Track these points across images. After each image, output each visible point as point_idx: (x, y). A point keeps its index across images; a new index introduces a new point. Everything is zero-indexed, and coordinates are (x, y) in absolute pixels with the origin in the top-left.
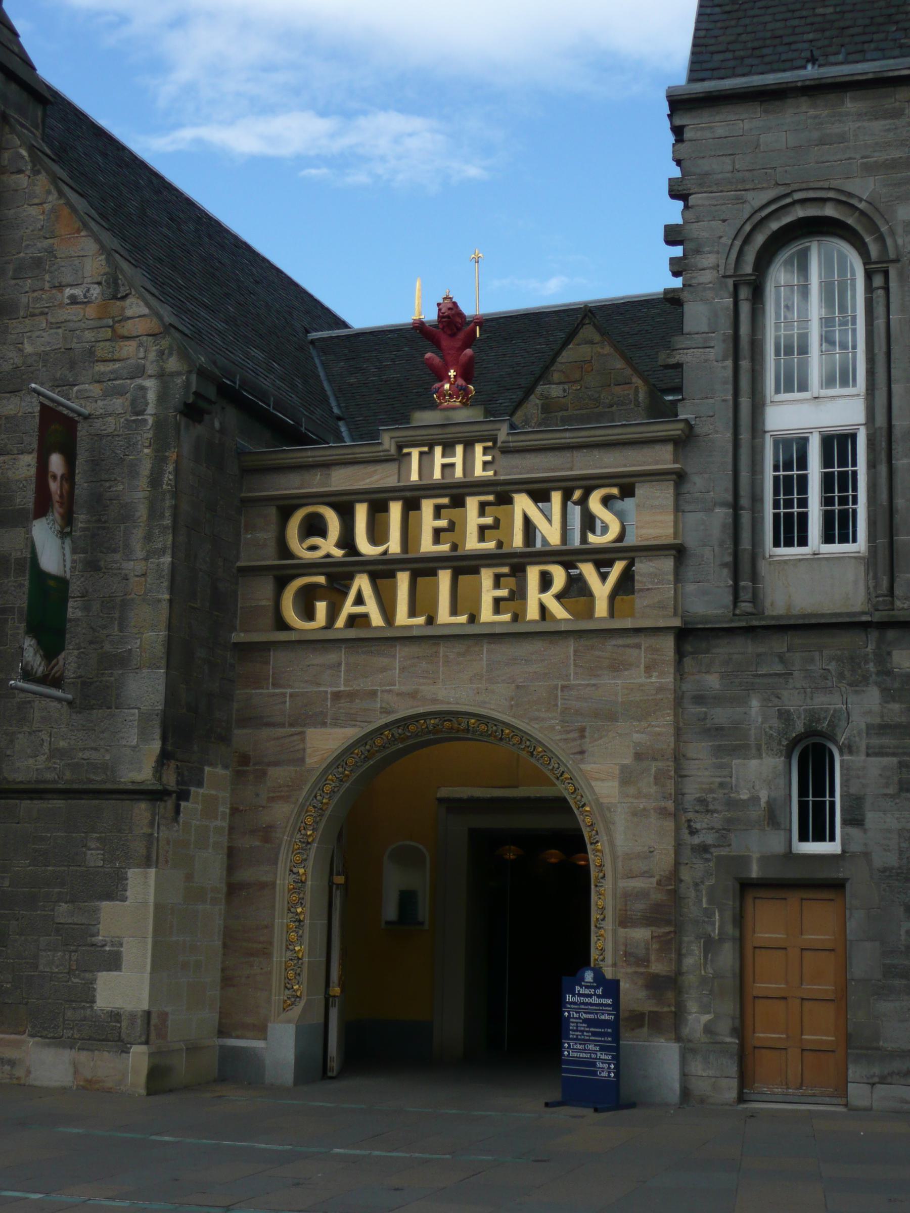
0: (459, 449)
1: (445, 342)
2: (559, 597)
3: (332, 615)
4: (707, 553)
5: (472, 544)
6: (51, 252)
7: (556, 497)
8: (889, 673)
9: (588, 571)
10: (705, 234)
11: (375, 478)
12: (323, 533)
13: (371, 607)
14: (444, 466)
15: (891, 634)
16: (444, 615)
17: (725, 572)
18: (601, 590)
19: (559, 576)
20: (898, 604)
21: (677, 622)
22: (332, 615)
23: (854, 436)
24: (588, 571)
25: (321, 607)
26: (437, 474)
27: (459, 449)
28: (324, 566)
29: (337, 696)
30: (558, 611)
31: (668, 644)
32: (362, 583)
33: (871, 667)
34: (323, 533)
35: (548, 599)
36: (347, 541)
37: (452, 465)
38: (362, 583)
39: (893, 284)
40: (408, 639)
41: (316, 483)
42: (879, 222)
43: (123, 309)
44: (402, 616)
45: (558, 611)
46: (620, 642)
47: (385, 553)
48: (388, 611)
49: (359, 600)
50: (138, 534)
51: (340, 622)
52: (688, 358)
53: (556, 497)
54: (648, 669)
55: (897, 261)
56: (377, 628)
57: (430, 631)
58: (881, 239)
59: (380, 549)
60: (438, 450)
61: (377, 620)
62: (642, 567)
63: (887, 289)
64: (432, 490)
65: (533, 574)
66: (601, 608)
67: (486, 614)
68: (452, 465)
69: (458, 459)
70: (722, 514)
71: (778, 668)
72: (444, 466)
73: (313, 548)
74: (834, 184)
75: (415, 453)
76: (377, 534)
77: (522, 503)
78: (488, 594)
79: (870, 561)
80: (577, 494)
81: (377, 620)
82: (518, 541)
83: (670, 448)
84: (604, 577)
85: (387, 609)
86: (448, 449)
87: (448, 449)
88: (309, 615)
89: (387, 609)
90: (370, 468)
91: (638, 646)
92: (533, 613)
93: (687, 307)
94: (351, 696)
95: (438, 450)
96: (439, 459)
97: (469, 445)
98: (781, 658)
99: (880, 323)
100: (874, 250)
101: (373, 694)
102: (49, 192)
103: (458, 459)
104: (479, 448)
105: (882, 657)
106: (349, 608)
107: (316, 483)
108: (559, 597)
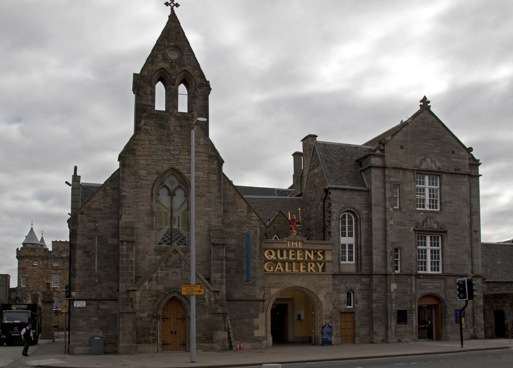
0: (296, 242)
1: (293, 223)
2: (313, 268)
3: (274, 269)
4: (335, 262)
5: (298, 258)
6: (235, 201)
7: (312, 252)
8: (361, 282)
9: (318, 264)
10: (334, 211)
11: (282, 246)
12: (272, 255)
13: (281, 268)
14: (294, 245)
15: (361, 276)
16: (294, 270)
17: (338, 265)
18: (320, 267)
19: (313, 265)
20: (362, 272)
21: (333, 273)
22: (274, 269)
23: (352, 245)
24: (318, 264)
25: (272, 268)
26: (293, 246)
27: (296, 242)
28: (272, 260)
29: (276, 283)
30: (314, 271)
31: (331, 276)
32: (279, 264)
33: (359, 281)
34: (272, 255)
35: (312, 268)
36: (276, 256)
37: (295, 245)
38: (279, 264)
39: (361, 223)
40: (288, 274)
41: (270, 246)
42: (359, 213)
43: (252, 215)
44: (287, 270)
45: (314, 271)
46: (324, 276)
47: (283, 259)
48: (284, 269)
49: (279, 267)
50: (257, 256)
51: (276, 270)
52: (332, 230)
53: (312, 252)
54: (328, 280)
55: (362, 219)
56: (283, 272)
57: (292, 273)
58: (359, 215)
59: (282, 258)
60: (293, 242)
61: (282, 270)
62: (327, 264)
63: (360, 223)
64: (292, 249)
65: (309, 264)
66: (320, 270)
67: (301, 270)
68: (295, 245)
69: (296, 244)
70: (337, 256)
71: (346, 280)
72: (294, 245)
73: (270, 257)
74: (353, 205)
75: (288, 242)
76: (282, 256)
77: (307, 252)
78: (302, 267)
79: (357, 264)
80: (316, 252)
81: (282, 270)
82: (306, 258)
83: (331, 245)
84: (320, 265)
85: (284, 268)
86: (294, 242)
87: (294, 242)
88: (270, 269)
89: (284, 268)
90: (280, 244)
91: (326, 277)
92: (309, 270)
93: (332, 222)
94: (279, 283)
95: (293, 242)
96: (293, 244)
97: (298, 242)
98: (346, 279)
99: (359, 228)
100: (358, 217)
101: (283, 283)
102: (233, 190)
103: (296, 244)
104: (300, 242)
105: (360, 279)
106: (277, 268)
107: (270, 246)
108: (313, 268)
